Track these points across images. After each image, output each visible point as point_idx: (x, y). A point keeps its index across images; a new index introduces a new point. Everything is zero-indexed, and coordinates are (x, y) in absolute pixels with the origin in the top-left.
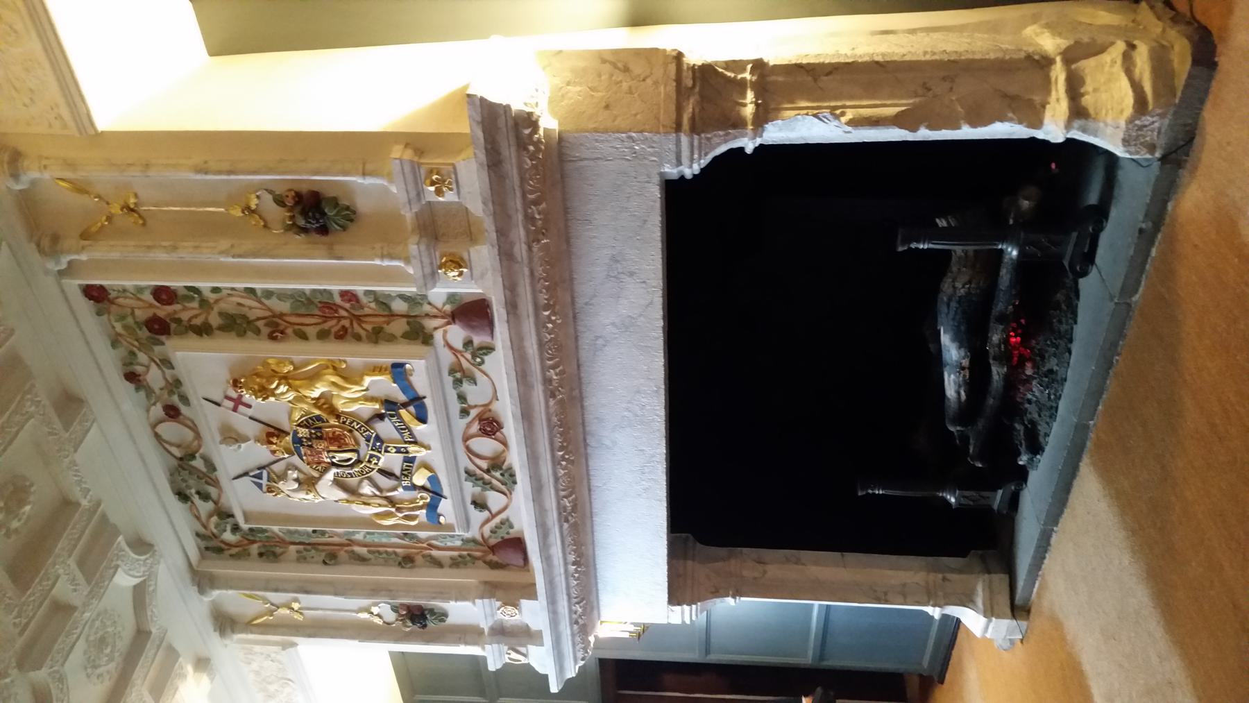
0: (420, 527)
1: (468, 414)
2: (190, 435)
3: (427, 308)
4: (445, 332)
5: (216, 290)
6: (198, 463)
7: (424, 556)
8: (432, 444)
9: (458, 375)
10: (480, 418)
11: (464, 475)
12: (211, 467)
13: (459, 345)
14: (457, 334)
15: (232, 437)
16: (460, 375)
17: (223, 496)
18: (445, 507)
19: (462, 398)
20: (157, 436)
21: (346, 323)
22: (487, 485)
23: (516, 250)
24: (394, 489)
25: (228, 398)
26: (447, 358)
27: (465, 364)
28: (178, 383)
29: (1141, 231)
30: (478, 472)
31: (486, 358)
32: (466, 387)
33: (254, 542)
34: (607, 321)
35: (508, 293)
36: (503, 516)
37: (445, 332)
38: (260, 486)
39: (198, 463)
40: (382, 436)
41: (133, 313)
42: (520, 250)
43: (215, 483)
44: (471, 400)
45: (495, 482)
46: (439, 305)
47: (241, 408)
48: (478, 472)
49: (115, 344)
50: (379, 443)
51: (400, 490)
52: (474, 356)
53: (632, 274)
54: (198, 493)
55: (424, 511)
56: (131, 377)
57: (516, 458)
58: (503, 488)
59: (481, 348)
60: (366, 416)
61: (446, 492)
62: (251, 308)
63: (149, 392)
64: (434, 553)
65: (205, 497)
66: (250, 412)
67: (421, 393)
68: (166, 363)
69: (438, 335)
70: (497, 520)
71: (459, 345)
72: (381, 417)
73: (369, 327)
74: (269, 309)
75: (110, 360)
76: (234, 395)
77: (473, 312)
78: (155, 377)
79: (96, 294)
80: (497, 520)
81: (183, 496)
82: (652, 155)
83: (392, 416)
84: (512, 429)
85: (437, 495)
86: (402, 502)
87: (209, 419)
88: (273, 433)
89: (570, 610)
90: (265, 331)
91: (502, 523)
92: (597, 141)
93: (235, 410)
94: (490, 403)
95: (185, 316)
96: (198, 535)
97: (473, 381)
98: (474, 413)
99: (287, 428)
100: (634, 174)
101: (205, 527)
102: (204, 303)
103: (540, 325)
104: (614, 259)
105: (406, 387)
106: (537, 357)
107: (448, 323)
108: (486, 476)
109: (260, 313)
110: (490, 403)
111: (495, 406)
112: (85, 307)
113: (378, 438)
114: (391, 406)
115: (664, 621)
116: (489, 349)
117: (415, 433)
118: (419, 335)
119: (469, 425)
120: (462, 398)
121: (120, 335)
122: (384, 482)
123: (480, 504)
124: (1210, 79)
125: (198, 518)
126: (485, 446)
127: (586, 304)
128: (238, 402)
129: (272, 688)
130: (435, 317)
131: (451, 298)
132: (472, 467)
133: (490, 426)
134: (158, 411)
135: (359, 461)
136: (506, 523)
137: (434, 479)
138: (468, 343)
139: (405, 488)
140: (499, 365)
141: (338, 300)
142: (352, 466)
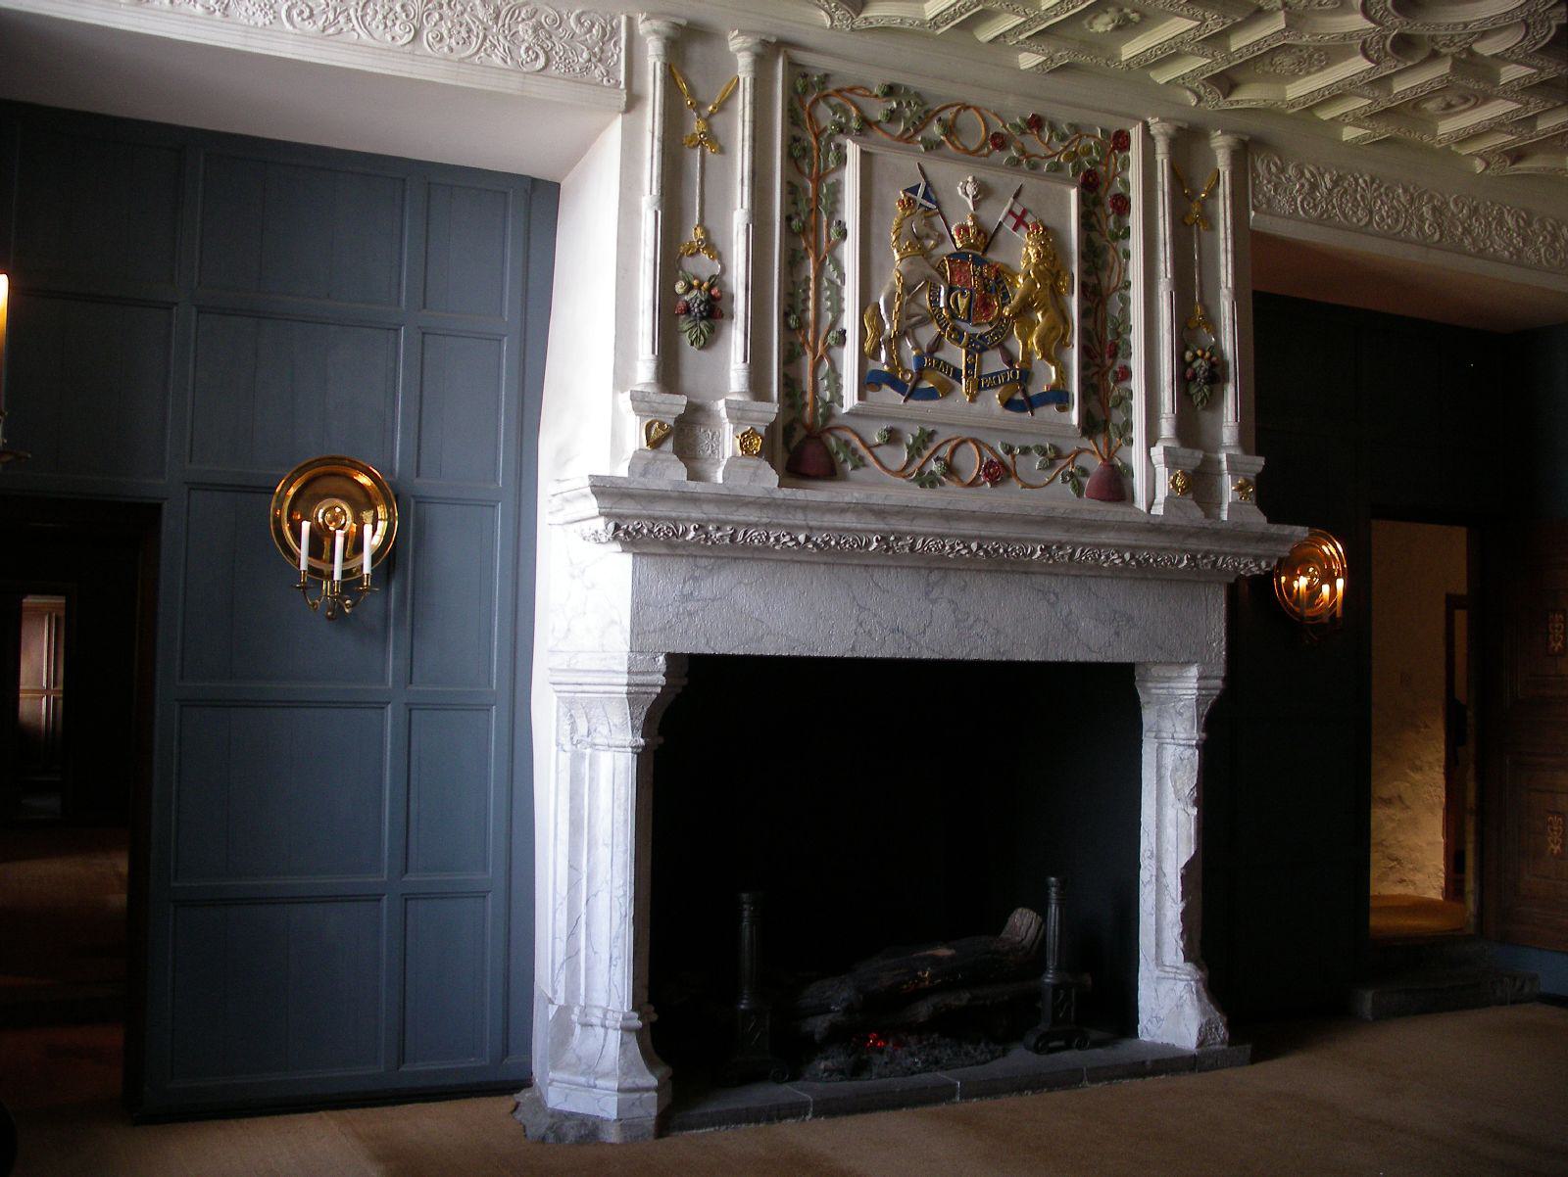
0: (863, 357)
1: (1007, 453)
2: (973, 147)
3: (1116, 440)
4: (1093, 453)
5: (1127, 255)
6: (935, 130)
7: (802, 345)
8: (977, 406)
9: (1051, 454)
10: (1002, 463)
11: (930, 429)
12: (932, 146)
13: (1081, 461)
14: (1094, 464)
15: (983, 192)
16: (1053, 456)
17: (886, 139)
18: (890, 397)
19: (1025, 451)
20: (967, 107)
21: (1098, 361)
22: (915, 451)
23: (1194, 541)
24: (917, 346)
25: (1025, 212)
26: (1069, 447)
27: (1062, 463)
28: (1034, 167)
29: (1144, 1063)
30: (932, 447)
31: (1069, 485)
32: (1037, 461)
33: (817, 137)
34: (1073, 607)
35: (1168, 528)
36: (870, 459)
37: (1093, 453)
38: (914, 190)
39: (935, 130)
40: (986, 355)
41: (1100, 163)
42: (1192, 544)
43: (906, 139)
44: (1021, 460)
45: (918, 462)
46: (1119, 454)
47: (1013, 221)
48: (932, 447)
49: (1075, 128)
50: (977, 347)
51: (914, 353)
52: (1072, 475)
53: (1117, 634)
54: (892, 111)
55: (886, 368)
56: (1036, 123)
57: (949, 496)
58: (914, 468)
59: (1079, 483)
60: (1007, 344)
61: (912, 403)
62: (1109, 277)
63: (1023, 133)
64: (808, 359)
65: (893, 116)
66: (1008, 226)
67: (1036, 411)
68: (1057, 168)
69: (1089, 444)
70: (863, 451)
71: (1081, 461)
72: (1010, 360)
73: (1095, 380)
74: (1109, 296)
75: (1064, 117)
76: (1029, 219)
77: (1116, 485)
78: (1034, 143)
79: (1121, 141)
80: (863, 451)
81: (891, 91)
82: (1210, 656)
83: (1014, 374)
84: (987, 498)
85: (913, 393)
86: (898, 348)
87: (1006, 181)
88: (986, 238)
89: (726, 523)
90: (1093, 280)
91: (862, 458)
92: (1219, 613)
93: (1011, 212)
94: (1019, 479)
95: (1098, 210)
96: (827, 76)
97: (1045, 468)
98: (1008, 459)
99: (992, 256)
100: (1196, 641)
101: (839, 91)
102: (1116, 237)
103: (1119, 549)
104: (1130, 619)
105: (1044, 399)
106: (1097, 541)
107: (1104, 459)
108: (926, 454)
109: (1105, 281)
110: (1019, 479)
111: (1014, 485)
112: (1115, 125)
113: (984, 349)
114: (1026, 376)
115: (1040, 658)
116: (1079, 490)
117: (991, 391)
118: (1091, 425)
119: (992, 450)
120: (1025, 451)
121: (1081, 137)
122: (928, 334)
123: (892, 437)
124: (1248, 1064)
125: (851, 90)
126: (970, 462)
127: (1090, 589)
128: (1020, 221)
129: (524, 30)
130: (1109, 448)
131: (1127, 472)
132: (938, 440)
133: (997, 473)
134: (998, 127)
135: (953, 316)
136: (859, 463)
137: (930, 395)
138: (1085, 472)
139: (919, 359)
140: (1059, 496)
141: (1120, 361)
142: (948, 306)
